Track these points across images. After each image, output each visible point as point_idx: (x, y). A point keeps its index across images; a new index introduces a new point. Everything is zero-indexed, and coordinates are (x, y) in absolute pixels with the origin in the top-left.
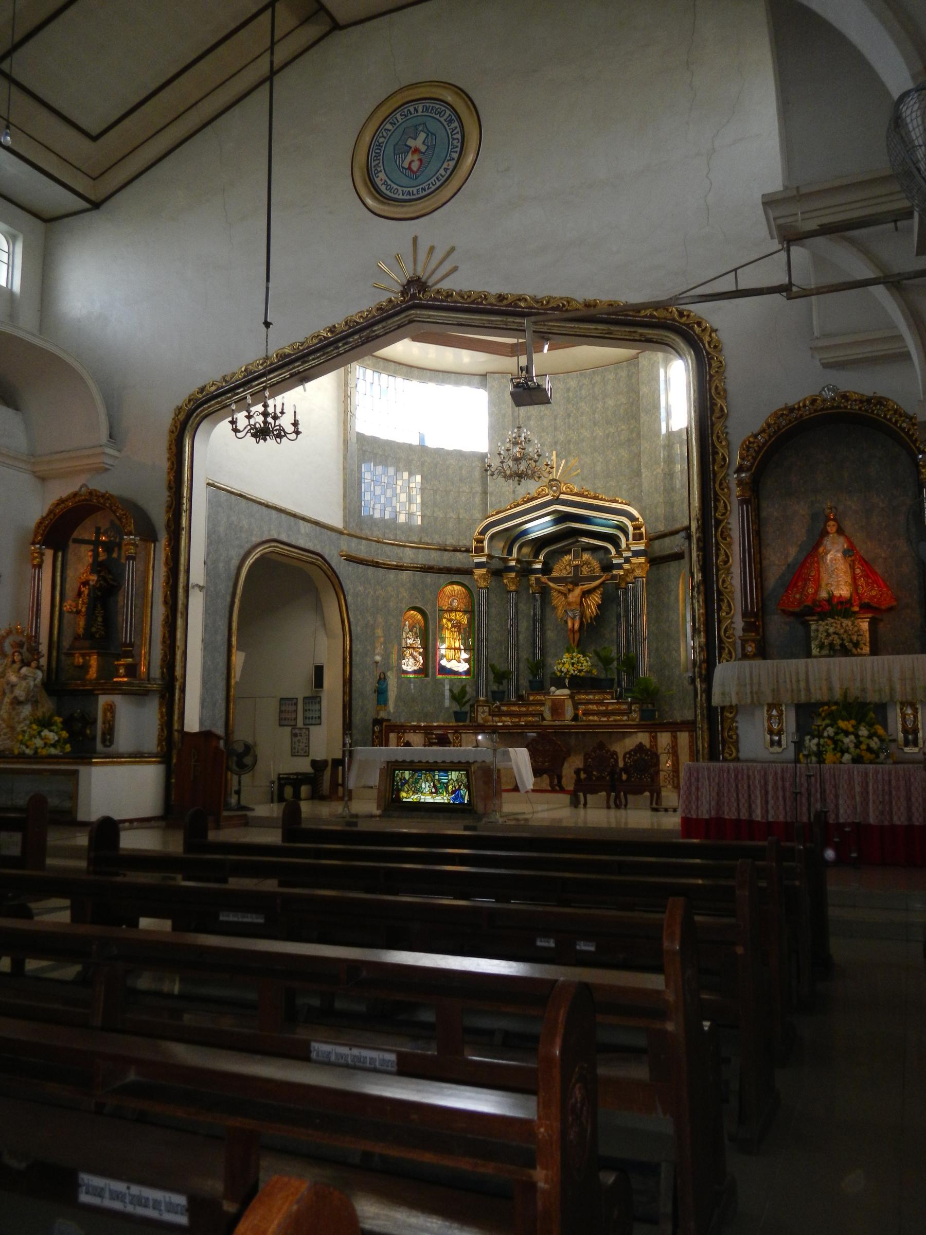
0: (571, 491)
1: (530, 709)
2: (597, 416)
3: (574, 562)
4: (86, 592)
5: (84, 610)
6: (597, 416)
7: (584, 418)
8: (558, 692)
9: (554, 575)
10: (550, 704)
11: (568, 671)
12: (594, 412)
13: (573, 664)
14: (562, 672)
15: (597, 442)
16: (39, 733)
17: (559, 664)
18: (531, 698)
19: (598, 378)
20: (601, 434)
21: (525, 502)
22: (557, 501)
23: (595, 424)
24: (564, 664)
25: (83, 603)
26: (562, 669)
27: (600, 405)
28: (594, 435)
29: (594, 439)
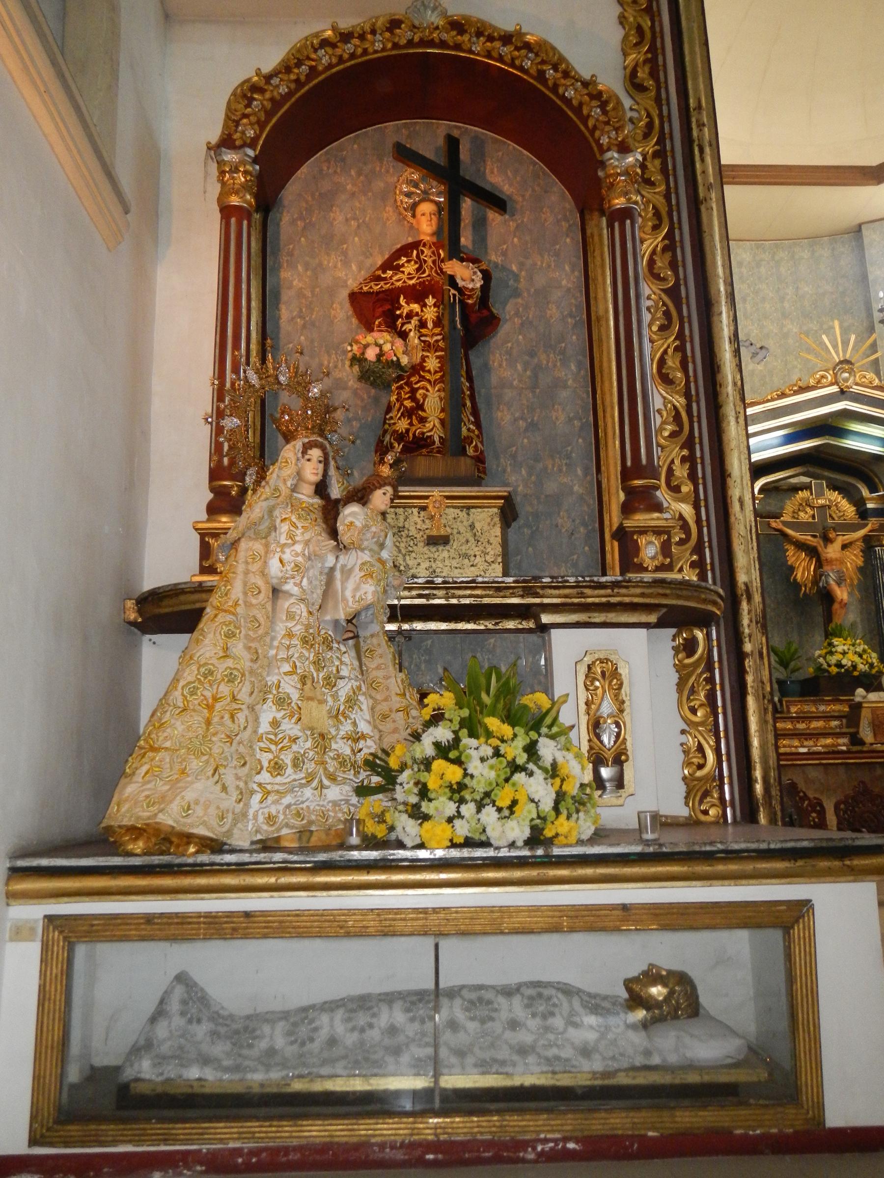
0: (871, 382)
1: (812, 726)
2: (786, 305)
3: (819, 501)
4: (430, 314)
5: (432, 363)
6: (786, 305)
7: (767, 306)
8: (873, 696)
9: (786, 518)
10: (870, 716)
11: (854, 667)
12: (782, 299)
13: (860, 656)
14: (839, 665)
15: (791, 341)
16: (531, 749)
17: (831, 653)
18: (793, 709)
19: (781, 254)
20: (795, 330)
21: (796, 393)
22: (843, 394)
23: (785, 316)
24: (844, 653)
25: (427, 346)
26: (844, 662)
27: (790, 291)
28: (785, 330)
29: (786, 336)
